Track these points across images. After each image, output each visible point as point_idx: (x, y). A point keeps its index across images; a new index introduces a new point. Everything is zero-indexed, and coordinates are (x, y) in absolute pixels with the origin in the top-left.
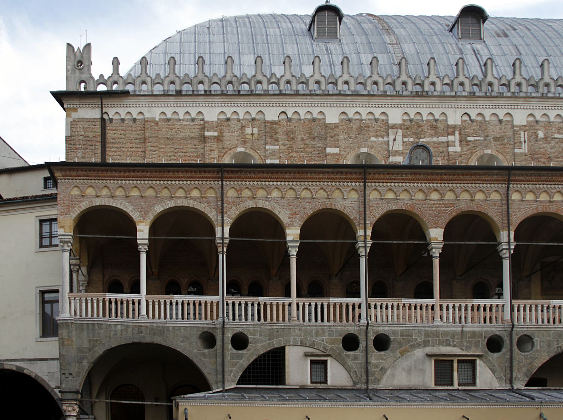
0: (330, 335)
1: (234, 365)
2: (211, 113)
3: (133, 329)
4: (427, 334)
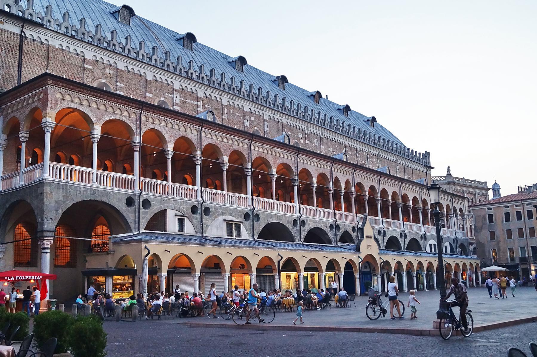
1: (143, 218)
2: (90, 54)
4: (224, 209)
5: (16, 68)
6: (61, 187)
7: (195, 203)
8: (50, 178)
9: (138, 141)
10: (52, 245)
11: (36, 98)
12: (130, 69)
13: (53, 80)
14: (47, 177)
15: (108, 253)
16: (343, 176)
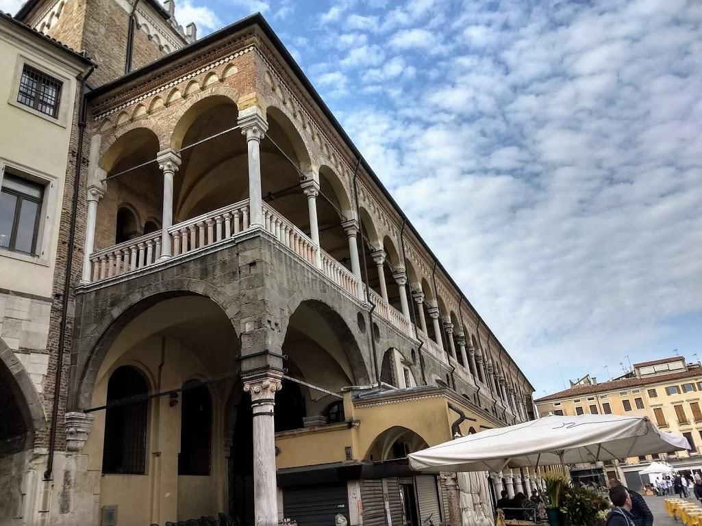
10: (278, 393)
15: (350, 425)
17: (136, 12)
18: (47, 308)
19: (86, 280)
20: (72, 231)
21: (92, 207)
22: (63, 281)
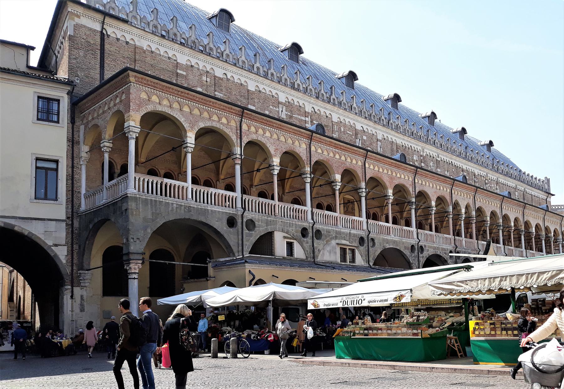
0: (296, 227)
2: (184, 57)
3: (185, 208)
4: (337, 232)
5: (98, 71)
6: (149, 203)
7: (305, 225)
8: (136, 191)
9: (239, 152)
11: (118, 100)
12: (229, 77)
13: (135, 77)
14: (132, 190)
16: (463, 198)
17: (105, 27)
18: (64, 224)
19: (83, 207)
20: (73, 183)
21: (84, 168)
22: (70, 210)
